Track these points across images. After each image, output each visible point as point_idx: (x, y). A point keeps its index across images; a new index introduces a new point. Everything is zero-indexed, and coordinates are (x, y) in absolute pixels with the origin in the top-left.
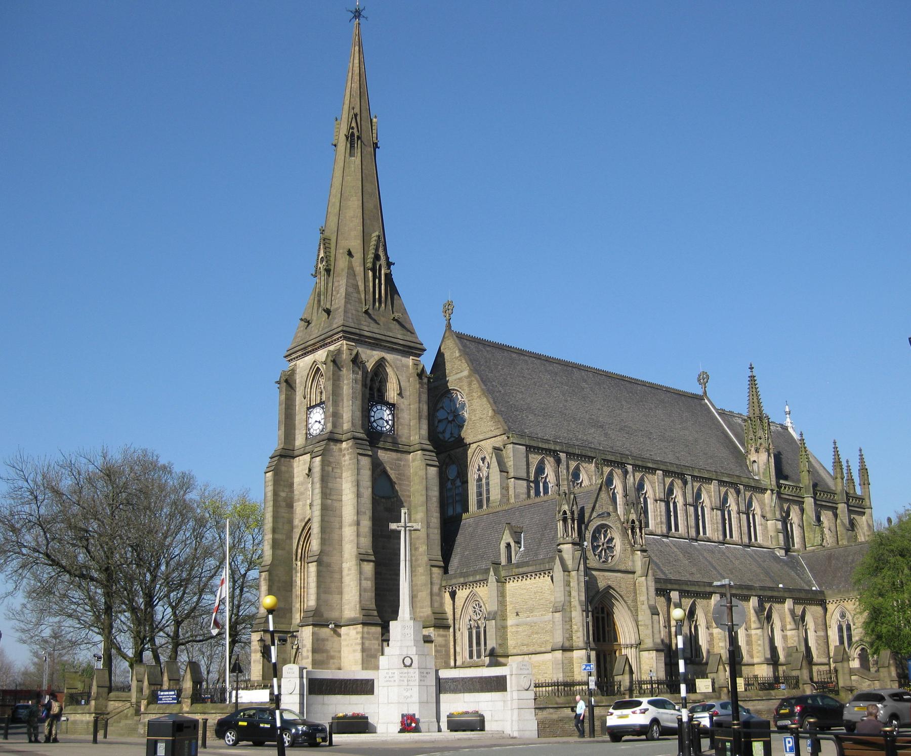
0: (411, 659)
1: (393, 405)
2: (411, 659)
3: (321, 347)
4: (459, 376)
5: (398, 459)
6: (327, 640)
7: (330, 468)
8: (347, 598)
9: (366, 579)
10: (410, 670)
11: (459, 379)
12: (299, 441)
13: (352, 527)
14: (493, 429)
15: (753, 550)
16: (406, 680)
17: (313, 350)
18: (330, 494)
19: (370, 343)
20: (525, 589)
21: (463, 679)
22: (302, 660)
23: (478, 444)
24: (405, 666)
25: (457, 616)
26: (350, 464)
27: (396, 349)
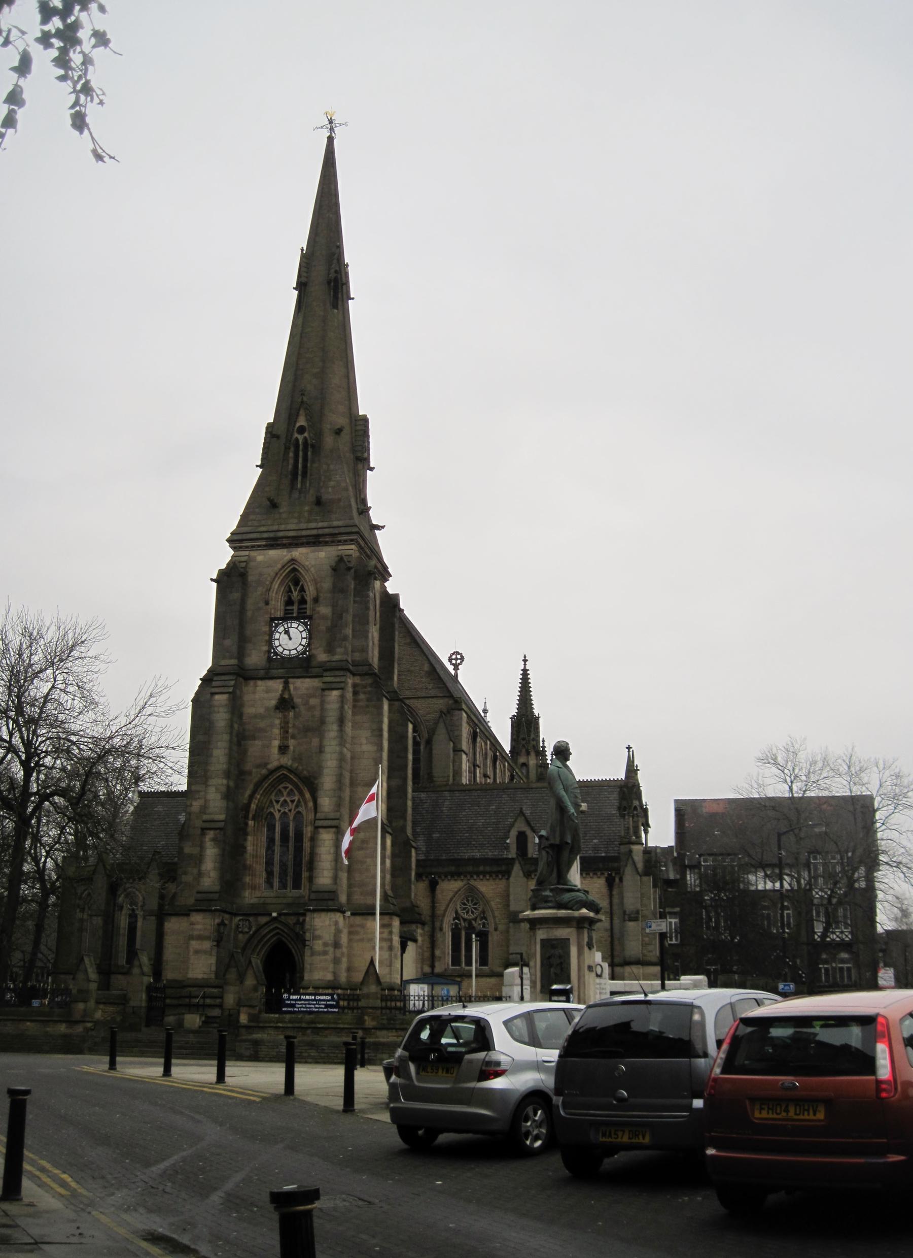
12: (255, 658)
14: (430, 687)
22: (312, 954)
25: (439, 912)
26: (367, 706)
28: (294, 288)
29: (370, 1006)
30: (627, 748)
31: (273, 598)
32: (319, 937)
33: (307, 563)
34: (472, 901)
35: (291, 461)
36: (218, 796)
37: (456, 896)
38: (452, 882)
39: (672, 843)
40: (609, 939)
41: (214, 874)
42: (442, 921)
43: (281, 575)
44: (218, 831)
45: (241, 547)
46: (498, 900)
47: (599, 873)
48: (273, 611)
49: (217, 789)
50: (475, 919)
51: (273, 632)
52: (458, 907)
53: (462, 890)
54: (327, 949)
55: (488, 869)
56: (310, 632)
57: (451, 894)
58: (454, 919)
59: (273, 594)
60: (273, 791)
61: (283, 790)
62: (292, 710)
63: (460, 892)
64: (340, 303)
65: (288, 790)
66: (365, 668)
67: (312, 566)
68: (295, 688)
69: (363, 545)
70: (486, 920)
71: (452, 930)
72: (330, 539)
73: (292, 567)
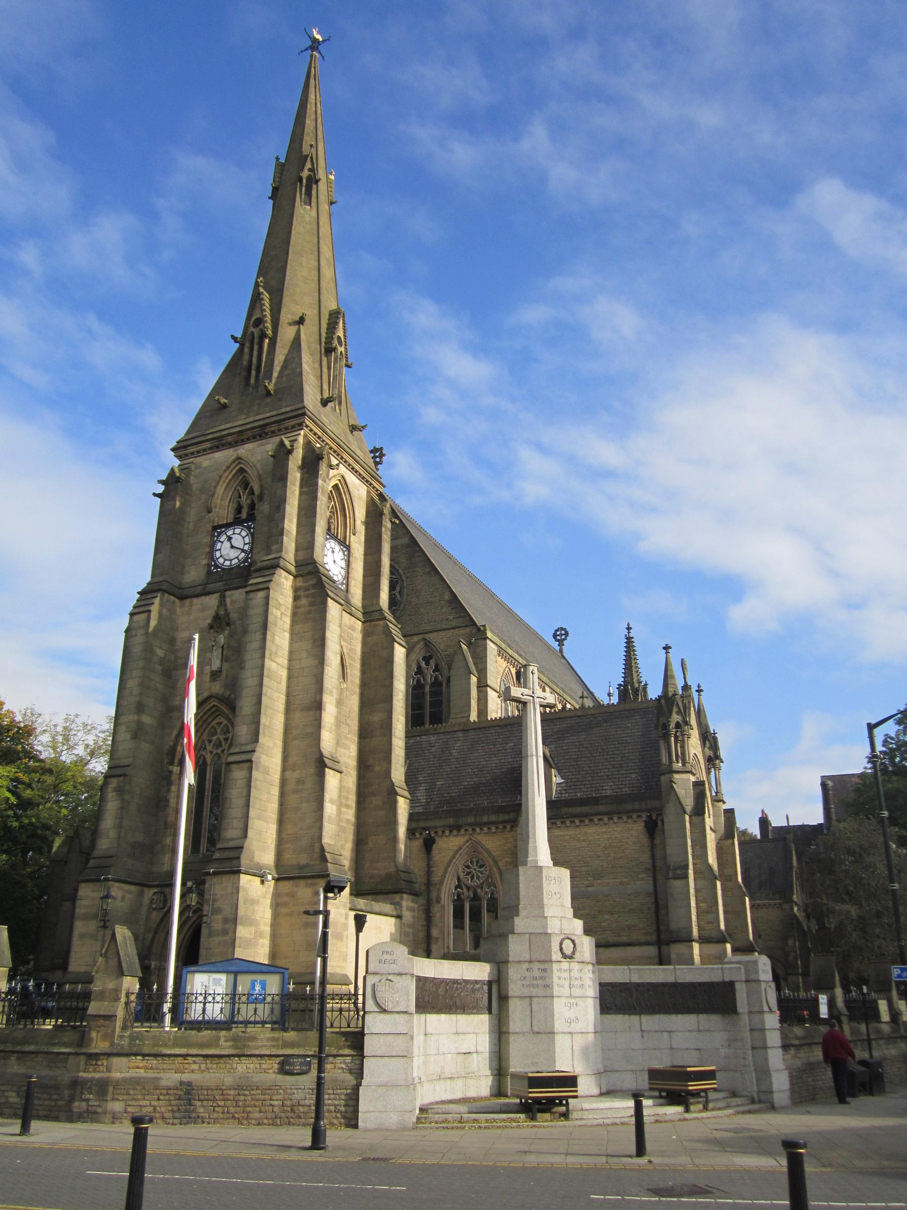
0: (573, 941)
2: (573, 941)
3: (254, 437)
7: (279, 614)
8: (290, 832)
9: (332, 801)
10: (575, 966)
13: (312, 713)
14: (451, 617)
16: (567, 984)
17: (236, 442)
20: (584, 840)
21: (638, 985)
22: (210, 935)
23: (422, 636)
24: (565, 956)
25: (436, 879)
26: (309, 612)
27: (356, 472)
28: (270, 198)
29: (102, 1013)
30: (664, 648)
31: (218, 506)
32: (218, 911)
33: (253, 460)
34: (477, 862)
35: (246, 357)
36: (129, 736)
37: (457, 857)
38: (452, 839)
39: (821, 821)
40: (653, 906)
41: (112, 834)
42: (439, 890)
43: (227, 477)
44: (122, 778)
45: (186, 455)
46: (507, 860)
47: (635, 816)
48: (216, 519)
49: (127, 727)
50: (481, 886)
51: (215, 542)
52: (460, 871)
53: (463, 848)
54: (227, 926)
55: (493, 818)
56: (252, 535)
57: (451, 854)
58: (456, 888)
59: (217, 500)
60: (205, 729)
61: (216, 726)
62: (228, 628)
63: (461, 851)
64: (314, 200)
65: (222, 726)
66: (310, 568)
67: (258, 461)
68: (232, 602)
69: (320, 434)
70: (495, 887)
71: (454, 901)
72: (276, 428)
73: (238, 468)
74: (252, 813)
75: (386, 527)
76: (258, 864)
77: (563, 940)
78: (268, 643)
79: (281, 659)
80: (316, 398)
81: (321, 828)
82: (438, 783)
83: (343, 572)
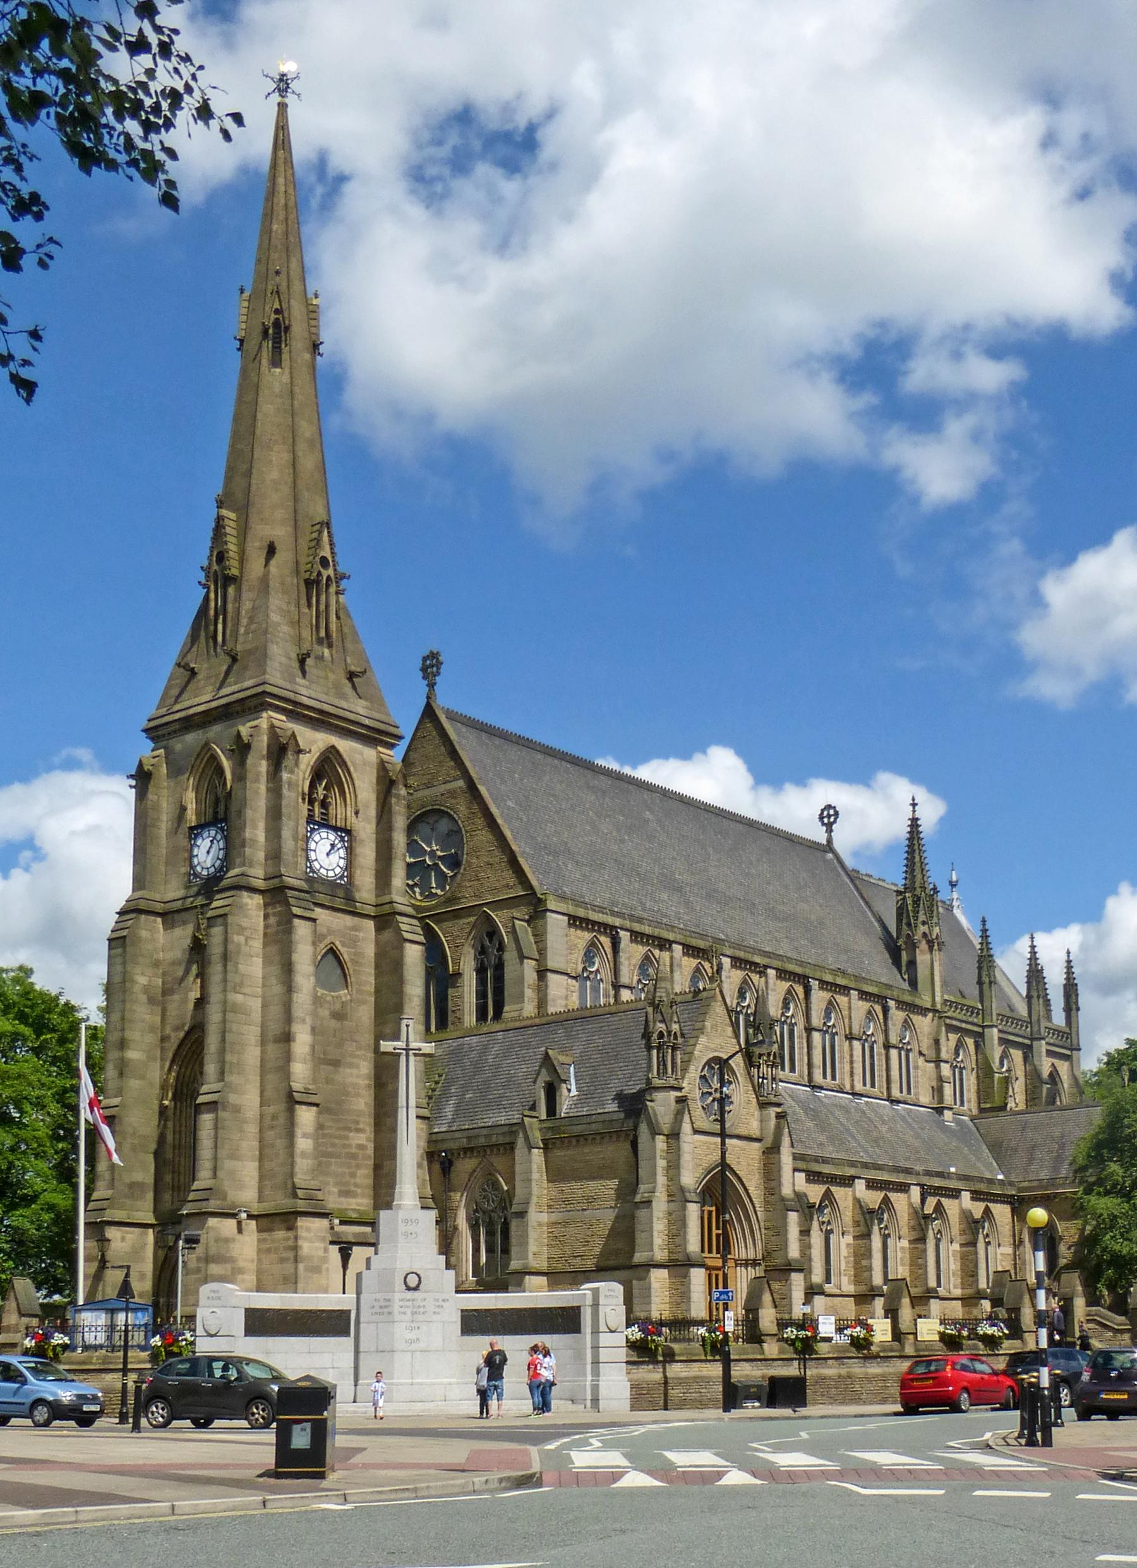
1: (348, 832)
4: (449, 786)
5: (355, 928)
6: (234, 1240)
9: (305, 1136)
11: (449, 791)
15: (905, 1109)
16: (409, 1311)
18: (241, 985)
19: (311, 718)
26: (277, 933)
38: (467, 1160)
66: (276, 881)
74: (222, 1153)
75: (398, 796)
76: (233, 1202)
77: (408, 1274)
78: (230, 976)
79: (249, 989)
80: (290, 659)
81: (292, 1165)
82: (468, 1096)
83: (342, 863)
